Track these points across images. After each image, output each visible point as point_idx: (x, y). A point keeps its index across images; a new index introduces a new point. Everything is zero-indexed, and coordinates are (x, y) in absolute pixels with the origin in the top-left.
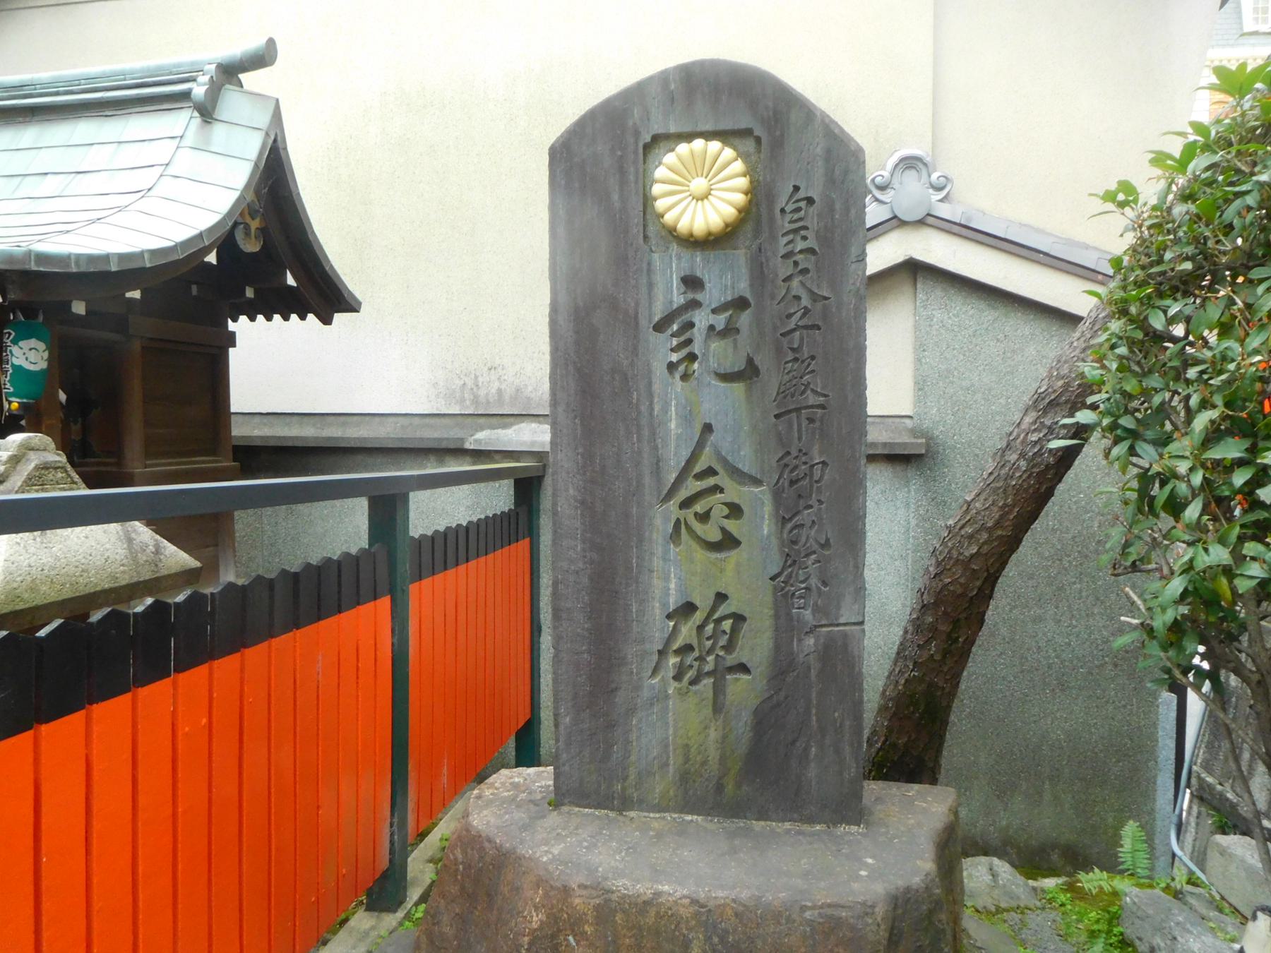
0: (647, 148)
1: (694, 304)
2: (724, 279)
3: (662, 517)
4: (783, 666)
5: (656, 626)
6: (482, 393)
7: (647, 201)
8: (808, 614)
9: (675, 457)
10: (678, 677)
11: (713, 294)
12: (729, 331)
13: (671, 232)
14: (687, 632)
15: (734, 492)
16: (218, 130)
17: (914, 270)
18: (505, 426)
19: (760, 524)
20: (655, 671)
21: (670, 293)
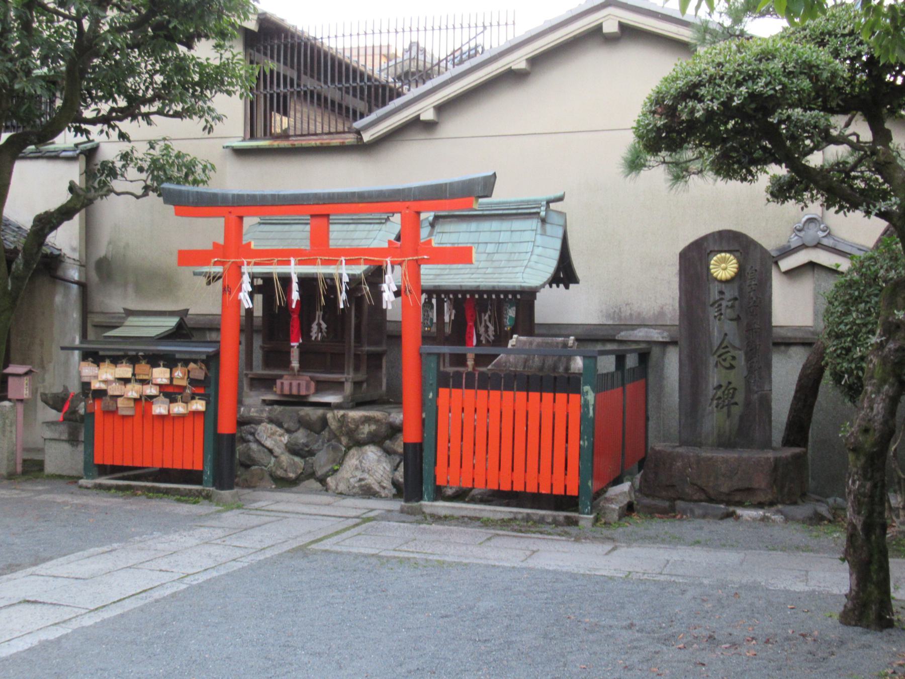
0: (708, 254)
1: (722, 299)
2: (730, 292)
3: (713, 360)
4: (748, 404)
5: (711, 392)
6: (623, 315)
7: (708, 269)
8: (755, 388)
9: (716, 342)
10: (717, 407)
11: (728, 295)
12: (732, 307)
13: (716, 279)
14: (719, 393)
15: (734, 353)
16: (548, 227)
17: (812, 266)
18: (633, 330)
19: (741, 361)
20: (710, 405)
21: (714, 295)
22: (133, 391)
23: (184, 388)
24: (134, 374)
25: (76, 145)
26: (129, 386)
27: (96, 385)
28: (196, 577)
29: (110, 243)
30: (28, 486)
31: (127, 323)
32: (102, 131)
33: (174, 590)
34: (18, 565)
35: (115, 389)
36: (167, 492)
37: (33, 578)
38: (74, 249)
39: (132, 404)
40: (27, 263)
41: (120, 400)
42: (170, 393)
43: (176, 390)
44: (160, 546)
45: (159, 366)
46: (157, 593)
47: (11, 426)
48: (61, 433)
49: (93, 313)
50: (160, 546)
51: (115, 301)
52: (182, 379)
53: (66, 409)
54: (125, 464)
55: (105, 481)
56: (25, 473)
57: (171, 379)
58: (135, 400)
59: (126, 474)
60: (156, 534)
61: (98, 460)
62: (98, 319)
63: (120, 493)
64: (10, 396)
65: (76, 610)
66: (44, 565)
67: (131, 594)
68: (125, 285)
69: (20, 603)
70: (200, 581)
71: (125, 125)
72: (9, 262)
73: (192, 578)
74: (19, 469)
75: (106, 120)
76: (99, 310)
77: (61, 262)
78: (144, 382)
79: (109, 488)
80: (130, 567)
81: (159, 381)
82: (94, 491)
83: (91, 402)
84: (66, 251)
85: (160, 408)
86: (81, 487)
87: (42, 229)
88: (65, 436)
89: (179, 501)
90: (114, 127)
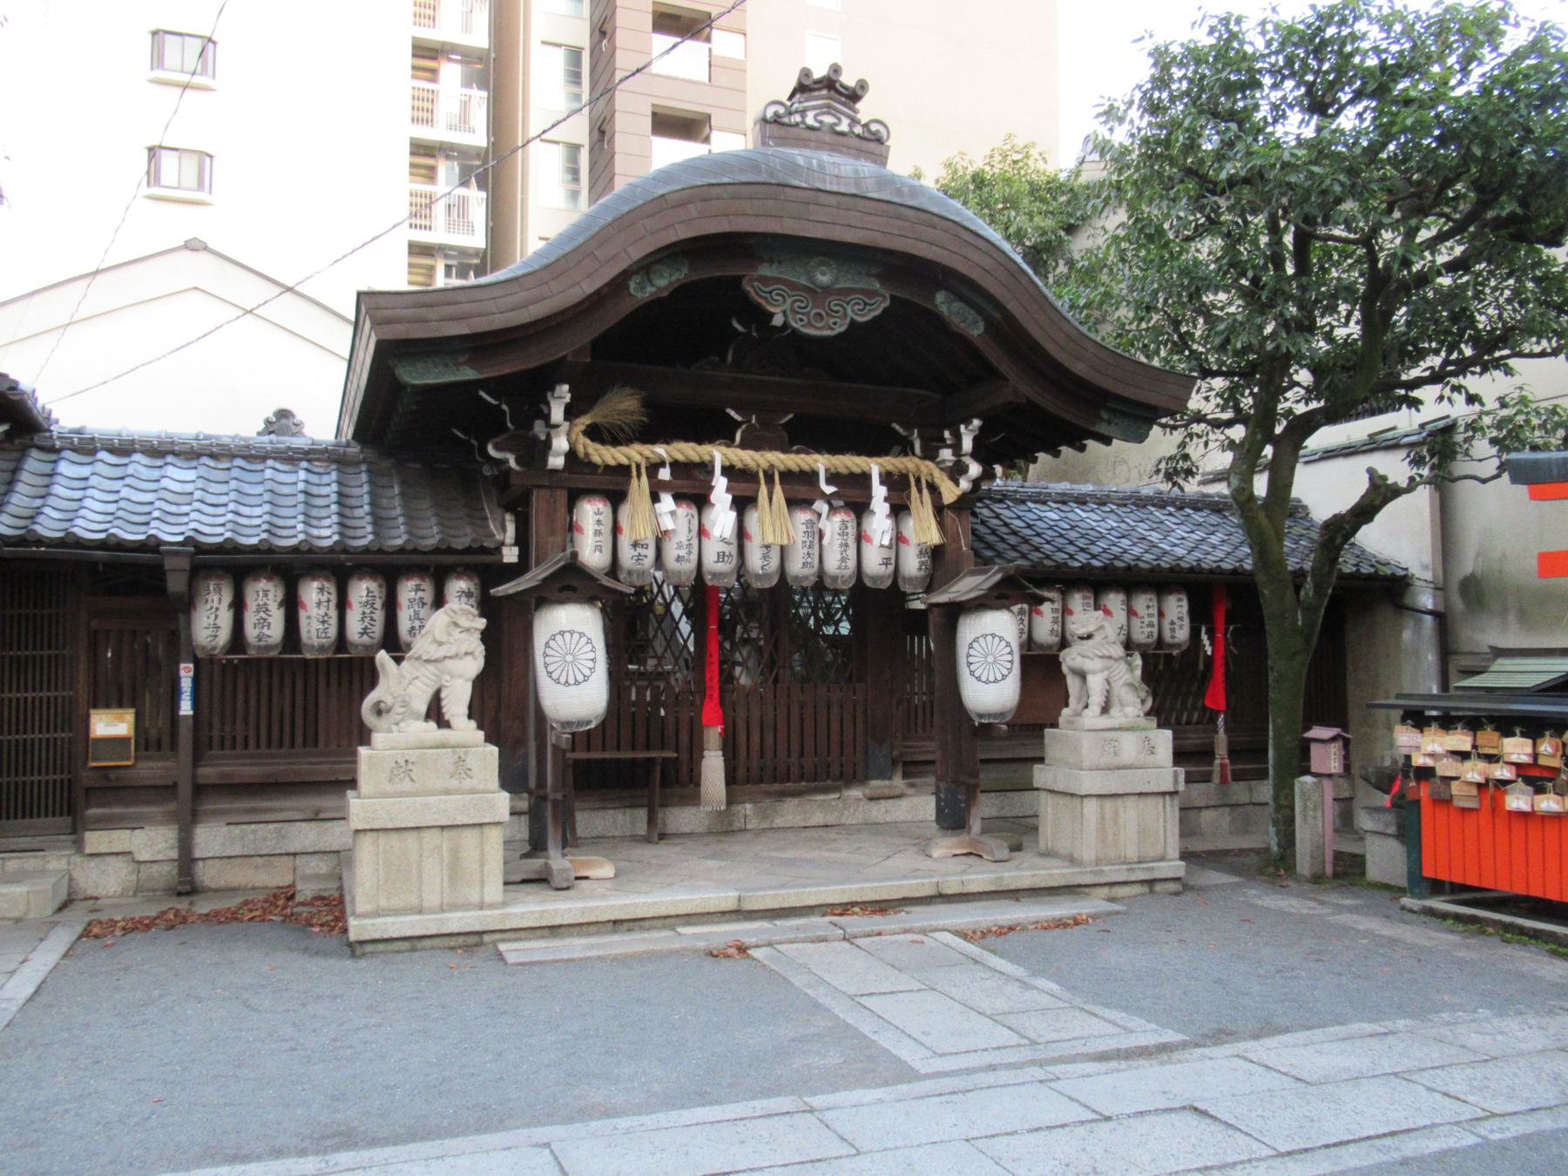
22: (1474, 772)
23: (1556, 771)
24: (1475, 747)
25: (1422, 426)
26: (1468, 764)
27: (1419, 760)
28: (1507, 1122)
29: (1478, 555)
30: (1334, 898)
31: (1494, 668)
32: (1441, 398)
33: (1451, 1143)
34: (1231, 1034)
35: (1446, 768)
36: (1536, 935)
37: (1240, 1062)
38: (1425, 567)
39: (1474, 792)
40: (1318, 588)
41: (1454, 784)
42: (1535, 777)
43: (1546, 775)
44: (1475, 1040)
45: (1513, 735)
46: (1413, 1144)
47: (1315, 810)
48: (1387, 825)
49: (1457, 653)
50: (1475, 1040)
51: (1486, 634)
52: (1553, 756)
53: (1395, 789)
54: (1469, 883)
55: (1437, 903)
56: (1336, 875)
57: (1535, 756)
58: (1479, 785)
59: (1479, 895)
60: (1483, 1012)
61: (1428, 873)
62: (1466, 662)
63: (1461, 928)
64: (1313, 769)
65: (1255, 1145)
66: (1269, 1042)
67: (1365, 1134)
68: (1504, 611)
69: (1184, 1108)
70: (1508, 1135)
71: (1472, 382)
72: (1298, 588)
73: (1496, 1123)
74: (1329, 870)
75: (1436, 377)
76: (1467, 649)
77: (1408, 585)
78: (1492, 759)
79: (1444, 916)
80: (1396, 1074)
81: (1514, 758)
82: (1422, 918)
83: (1413, 784)
84: (1415, 570)
85: (1518, 801)
86: (1403, 908)
87: (1332, 539)
88: (1392, 830)
89: (1554, 953)
90: (1457, 389)
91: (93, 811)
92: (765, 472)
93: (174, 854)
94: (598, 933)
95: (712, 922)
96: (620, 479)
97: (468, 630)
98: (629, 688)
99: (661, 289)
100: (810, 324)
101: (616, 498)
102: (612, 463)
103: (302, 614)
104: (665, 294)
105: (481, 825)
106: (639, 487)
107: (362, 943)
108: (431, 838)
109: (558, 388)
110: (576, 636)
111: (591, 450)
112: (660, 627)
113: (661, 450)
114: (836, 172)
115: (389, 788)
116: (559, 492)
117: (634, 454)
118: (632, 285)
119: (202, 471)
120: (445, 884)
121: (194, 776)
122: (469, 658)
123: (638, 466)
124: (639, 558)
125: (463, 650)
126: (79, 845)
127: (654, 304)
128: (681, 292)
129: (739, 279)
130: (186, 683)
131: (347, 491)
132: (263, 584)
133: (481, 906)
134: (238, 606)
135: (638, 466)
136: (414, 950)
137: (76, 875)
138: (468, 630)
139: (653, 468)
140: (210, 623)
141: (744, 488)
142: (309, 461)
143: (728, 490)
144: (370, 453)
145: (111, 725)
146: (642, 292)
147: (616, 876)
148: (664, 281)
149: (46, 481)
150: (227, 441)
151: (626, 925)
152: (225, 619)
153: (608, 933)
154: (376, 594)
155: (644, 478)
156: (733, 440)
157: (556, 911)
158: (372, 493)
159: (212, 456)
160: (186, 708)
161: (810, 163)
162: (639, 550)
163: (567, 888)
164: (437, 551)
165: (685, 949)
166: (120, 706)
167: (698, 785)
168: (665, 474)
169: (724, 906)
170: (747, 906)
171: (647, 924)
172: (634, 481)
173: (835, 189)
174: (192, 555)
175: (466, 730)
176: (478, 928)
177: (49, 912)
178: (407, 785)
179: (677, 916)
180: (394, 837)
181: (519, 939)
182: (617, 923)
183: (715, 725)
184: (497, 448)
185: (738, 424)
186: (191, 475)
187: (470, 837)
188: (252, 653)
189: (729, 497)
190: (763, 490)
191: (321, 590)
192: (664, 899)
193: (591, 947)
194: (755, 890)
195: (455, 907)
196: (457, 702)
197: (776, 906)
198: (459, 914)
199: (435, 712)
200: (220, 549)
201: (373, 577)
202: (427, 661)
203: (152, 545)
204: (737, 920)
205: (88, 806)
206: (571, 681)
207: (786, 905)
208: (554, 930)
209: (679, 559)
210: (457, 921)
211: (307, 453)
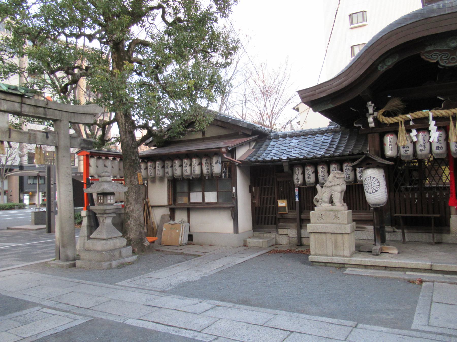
91: (280, 224)
92: (452, 116)
93: (296, 236)
94: (380, 270)
95: (421, 272)
96: (394, 127)
97: (339, 178)
98: (426, 193)
99: (389, 66)
100: (449, 63)
101: (396, 133)
102: (392, 122)
103: (319, 175)
104: (391, 67)
105: (342, 233)
106: (402, 129)
107: (312, 262)
108: (329, 236)
109: (368, 103)
110: (372, 178)
111: (384, 120)
112: (437, 172)
113: (409, 116)
114: (451, 5)
115: (317, 221)
116: (375, 134)
117: (400, 118)
118: (379, 67)
119: (300, 140)
120: (334, 249)
121: (300, 217)
122: (338, 186)
123: (401, 122)
124: (406, 152)
125: (336, 184)
126: (277, 231)
127: (387, 72)
128: (397, 66)
129: (419, 54)
130: (297, 193)
131: (334, 140)
132: (308, 168)
133: (344, 256)
134: (303, 173)
135: (401, 122)
136: (326, 266)
137: (277, 238)
138: (339, 178)
139: (407, 122)
140: (298, 178)
141: (442, 124)
142: (327, 133)
143: (435, 125)
144: (343, 129)
145: (282, 204)
146: (382, 69)
147: (399, 253)
148: (390, 63)
149: (266, 147)
150: (308, 131)
151: (389, 268)
152: (301, 177)
153: (383, 270)
154: (336, 168)
155: (403, 125)
156: (441, 107)
157: (366, 261)
158: (340, 140)
159: (304, 135)
160: (297, 200)
161: (439, 6)
162: (405, 149)
163: (377, 255)
164: (349, 155)
165: (400, 278)
166: (284, 199)
167: (449, 226)
168: (411, 123)
169: (425, 267)
170: (434, 268)
171: (397, 269)
172: (400, 127)
173: (450, 12)
174: (288, 162)
175: (340, 205)
176: (342, 262)
177: (267, 246)
178: (322, 221)
179: (407, 268)
180: (319, 235)
181: (355, 268)
182: (386, 267)
183: (454, 206)
184: (356, 124)
185: (443, 101)
186: (297, 141)
187: (340, 236)
188: (308, 186)
189: (436, 127)
190: (452, 122)
191: (322, 168)
192: (402, 262)
193: (373, 273)
194: (439, 263)
195: (337, 256)
196: (338, 197)
197: (446, 269)
198: (337, 258)
199: (331, 202)
200: (295, 160)
201: (335, 164)
202: (328, 187)
203: (280, 160)
204: (431, 273)
205: (279, 223)
206: (371, 192)
207: (451, 270)
208: (366, 267)
209: (421, 150)
210: (336, 260)
211: (326, 131)
